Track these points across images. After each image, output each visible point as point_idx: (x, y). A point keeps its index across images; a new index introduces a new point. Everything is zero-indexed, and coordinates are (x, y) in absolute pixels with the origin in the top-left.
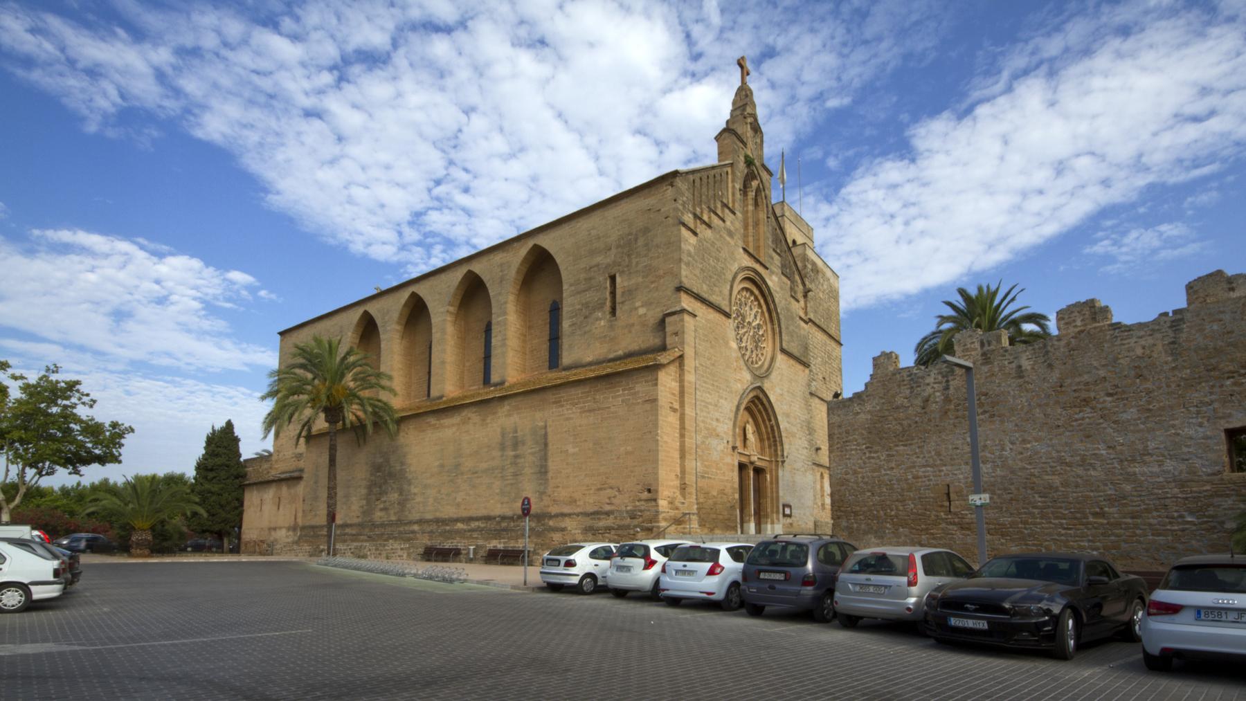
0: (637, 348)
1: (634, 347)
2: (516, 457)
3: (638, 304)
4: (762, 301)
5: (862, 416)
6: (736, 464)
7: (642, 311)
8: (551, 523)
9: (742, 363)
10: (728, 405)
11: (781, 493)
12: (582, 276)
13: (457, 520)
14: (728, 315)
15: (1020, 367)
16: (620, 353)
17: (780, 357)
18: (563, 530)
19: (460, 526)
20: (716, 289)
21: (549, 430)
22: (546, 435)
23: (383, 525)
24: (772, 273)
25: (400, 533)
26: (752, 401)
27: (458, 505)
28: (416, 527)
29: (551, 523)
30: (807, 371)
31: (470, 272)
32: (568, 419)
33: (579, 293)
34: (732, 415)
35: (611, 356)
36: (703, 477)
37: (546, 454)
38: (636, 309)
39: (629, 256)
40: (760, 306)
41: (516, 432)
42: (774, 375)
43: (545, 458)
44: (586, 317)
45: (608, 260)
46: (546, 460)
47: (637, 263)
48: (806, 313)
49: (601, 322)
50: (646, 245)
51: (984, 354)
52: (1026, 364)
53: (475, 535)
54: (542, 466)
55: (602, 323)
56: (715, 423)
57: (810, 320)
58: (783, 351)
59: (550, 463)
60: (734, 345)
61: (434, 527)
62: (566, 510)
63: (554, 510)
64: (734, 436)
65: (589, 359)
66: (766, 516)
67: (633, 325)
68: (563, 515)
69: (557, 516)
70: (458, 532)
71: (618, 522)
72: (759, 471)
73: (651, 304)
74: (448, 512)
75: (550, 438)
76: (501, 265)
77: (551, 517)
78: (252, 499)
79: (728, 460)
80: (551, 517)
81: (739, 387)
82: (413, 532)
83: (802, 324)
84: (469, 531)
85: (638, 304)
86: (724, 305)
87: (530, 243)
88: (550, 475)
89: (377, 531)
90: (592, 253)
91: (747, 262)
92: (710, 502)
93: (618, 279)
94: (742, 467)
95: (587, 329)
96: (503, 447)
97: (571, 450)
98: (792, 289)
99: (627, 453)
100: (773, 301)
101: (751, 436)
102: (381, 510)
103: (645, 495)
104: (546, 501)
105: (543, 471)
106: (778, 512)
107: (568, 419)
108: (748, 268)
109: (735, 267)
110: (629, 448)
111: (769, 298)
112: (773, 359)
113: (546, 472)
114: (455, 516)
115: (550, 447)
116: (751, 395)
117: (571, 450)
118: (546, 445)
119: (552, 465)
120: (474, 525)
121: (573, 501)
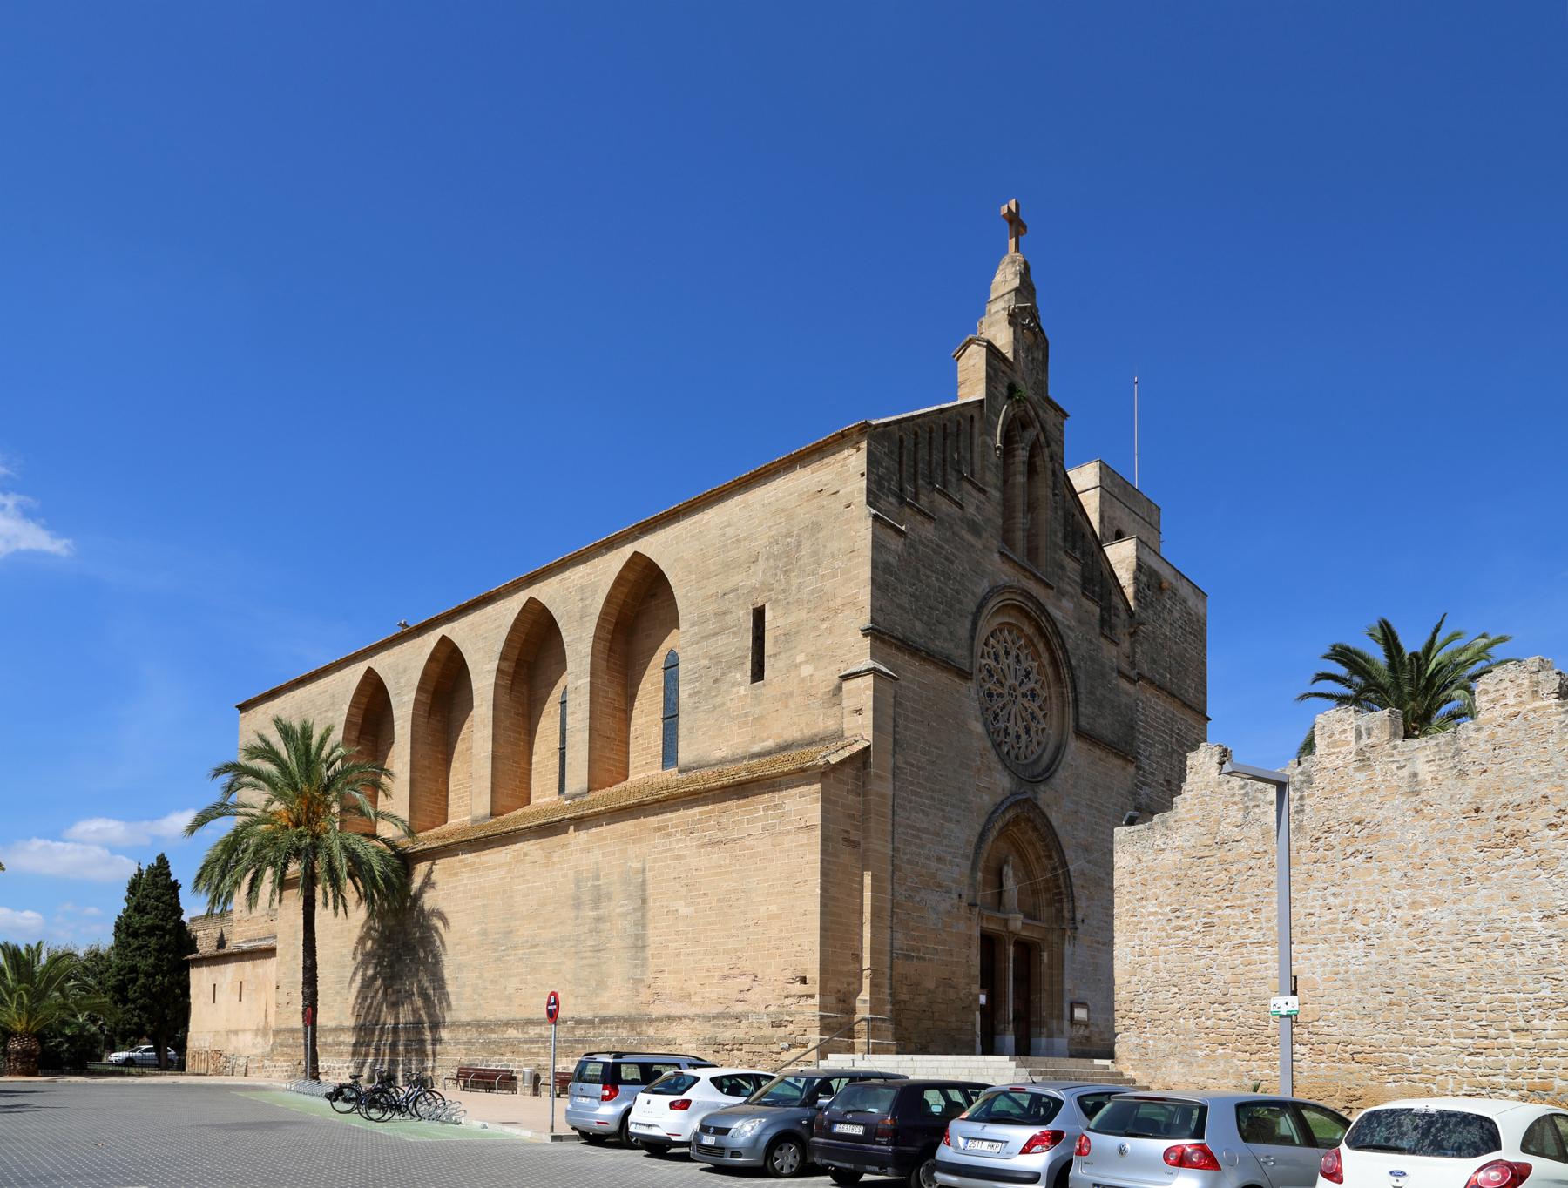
0: (797, 735)
3: (800, 658)
4: (1041, 646)
5: (1168, 855)
6: (977, 933)
7: (806, 670)
8: (651, 1031)
9: (993, 756)
11: (1068, 985)
12: (712, 607)
13: (507, 1024)
14: (965, 675)
15: (1415, 775)
16: (770, 744)
17: (1074, 745)
19: (512, 1033)
20: (943, 629)
22: (644, 882)
24: (1062, 594)
26: (1015, 821)
27: (510, 999)
29: (651, 1031)
30: (1132, 769)
31: (532, 601)
32: (678, 857)
34: (970, 851)
35: (756, 748)
36: (908, 957)
38: (797, 666)
40: (1037, 655)
42: (1061, 776)
44: (715, 681)
45: (754, 581)
48: (1133, 664)
50: (815, 554)
51: (1360, 752)
52: (1425, 772)
53: (535, 1048)
54: (637, 937)
56: (934, 865)
57: (1141, 677)
58: (1080, 734)
59: (650, 932)
60: (978, 727)
61: (472, 1034)
62: (676, 1010)
63: (656, 1010)
64: (972, 885)
66: (1041, 1024)
67: (791, 694)
69: (659, 1020)
70: (509, 1043)
71: (754, 1032)
72: (1027, 950)
73: (821, 657)
75: (650, 890)
76: (582, 588)
77: (651, 1021)
79: (962, 927)
81: (987, 801)
83: (1124, 684)
84: (525, 1042)
86: (960, 655)
90: (728, 567)
91: (1006, 574)
92: (922, 999)
94: (990, 944)
95: (718, 700)
97: (683, 911)
98: (1104, 622)
99: (771, 917)
100: (1063, 646)
101: (1010, 883)
104: (645, 995)
106: (1061, 1017)
107: (678, 857)
108: (1008, 588)
109: (983, 587)
110: (774, 908)
111: (1055, 641)
112: (1059, 750)
114: (505, 1017)
115: (650, 904)
116: (1011, 814)
121: (686, 997)
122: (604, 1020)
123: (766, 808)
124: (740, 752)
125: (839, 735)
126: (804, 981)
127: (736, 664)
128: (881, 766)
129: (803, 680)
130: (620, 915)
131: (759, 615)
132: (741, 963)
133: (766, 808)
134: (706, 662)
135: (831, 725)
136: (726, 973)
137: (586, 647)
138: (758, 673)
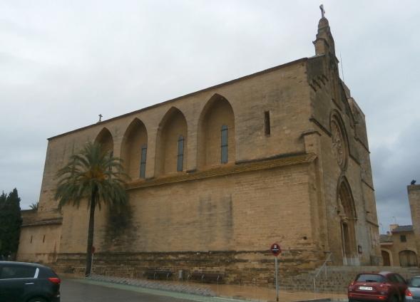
1: (283, 152)
2: (211, 215)
3: (284, 128)
7: (287, 132)
10: (334, 186)
18: (245, 261)
19: (171, 257)
21: (233, 199)
22: (231, 203)
23: (116, 255)
25: (128, 260)
28: (140, 257)
29: (236, 257)
33: (246, 120)
35: (268, 157)
37: (231, 215)
38: (284, 130)
39: (277, 101)
41: (210, 200)
43: (231, 216)
44: (250, 134)
46: (231, 218)
47: (283, 106)
49: (261, 137)
53: (182, 263)
55: (261, 138)
61: (152, 257)
63: (238, 249)
65: (253, 158)
67: (281, 139)
68: (245, 252)
69: (240, 252)
70: (170, 261)
74: (165, 249)
75: (234, 204)
77: (236, 253)
78: (26, 235)
80: (236, 253)
82: (137, 260)
85: (284, 128)
87: (213, 93)
88: (235, 227)
89: (112, 258)
93: (271, 114)
96: (201, 209)
102: (115, 245)
103: (303, 241)
104: (232, 243)
105: (230, 225)
108: (335, 110)
110: (290, 212)
113: (231, 225)
114: (167, 251)
115: (234, 209)
117: (249, 212)
118: (231, 208)
119: (236, 221)
120: (180, 256)
121: (251, 244)
122: (214, 253)
123: (284, 177)
124: (261, 158)
125: (304, 153)
126: (305, 238)
127: (260, 129)
128: (321, 162)
129: (286, 135)
130: (222, 214)
131: (267, 114)
132: (276, 232)
133: (284, 177)
134: (245, 128)
135: (299, 149)
136: (270, 235)
137: (196, 122)
138: (268, 132)
